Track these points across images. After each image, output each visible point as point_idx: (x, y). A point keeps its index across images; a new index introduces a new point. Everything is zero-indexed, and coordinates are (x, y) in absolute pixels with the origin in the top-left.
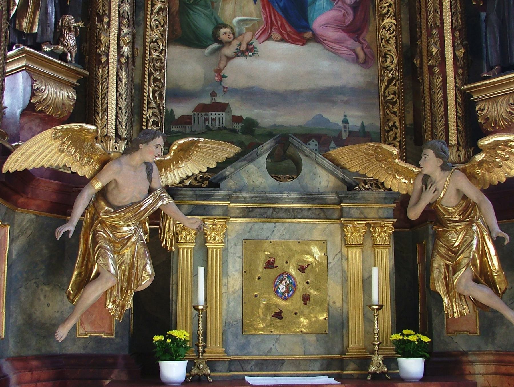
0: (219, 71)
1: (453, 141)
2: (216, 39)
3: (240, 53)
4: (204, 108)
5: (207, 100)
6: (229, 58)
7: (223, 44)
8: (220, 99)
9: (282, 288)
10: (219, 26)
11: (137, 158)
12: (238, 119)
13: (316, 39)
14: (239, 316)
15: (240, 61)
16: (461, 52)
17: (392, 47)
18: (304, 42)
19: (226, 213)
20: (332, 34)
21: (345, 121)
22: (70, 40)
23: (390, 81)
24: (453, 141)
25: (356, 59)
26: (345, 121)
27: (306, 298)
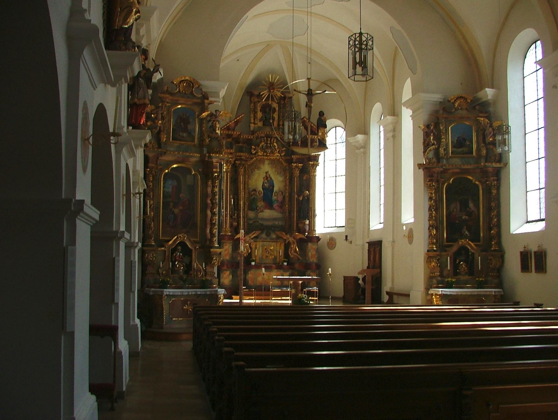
0: (257, 215)
1: (295, 230)
2: (257, 209)
3: (261, 212)
4: (255, 222)
5: (255, 220)
6: (259, 213)
7: (258, 210)
8: (257, 220)
9: (267, 253)
10: (257, 207)
11: (249, 235)
12: (260, 224)
13: (274, 209)
14: (261, 256)
15: (261, 213)
16: (297, 215)
17: (287, 211)
18: (272, 210)
19: (259, 241)
20: (277, 208)
21: (279, 224)
22: (236, 215)
23: (287, 217)
24: (295, 230)
25: (281, 213)
26: (279, 224)
27: (271, 254)
